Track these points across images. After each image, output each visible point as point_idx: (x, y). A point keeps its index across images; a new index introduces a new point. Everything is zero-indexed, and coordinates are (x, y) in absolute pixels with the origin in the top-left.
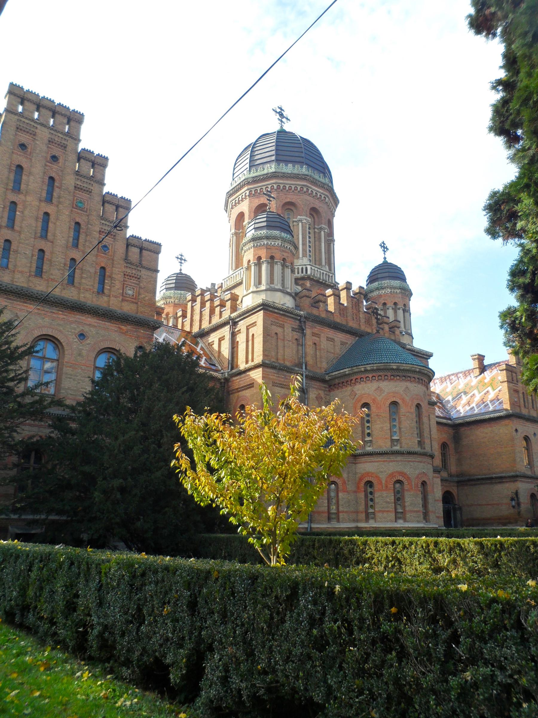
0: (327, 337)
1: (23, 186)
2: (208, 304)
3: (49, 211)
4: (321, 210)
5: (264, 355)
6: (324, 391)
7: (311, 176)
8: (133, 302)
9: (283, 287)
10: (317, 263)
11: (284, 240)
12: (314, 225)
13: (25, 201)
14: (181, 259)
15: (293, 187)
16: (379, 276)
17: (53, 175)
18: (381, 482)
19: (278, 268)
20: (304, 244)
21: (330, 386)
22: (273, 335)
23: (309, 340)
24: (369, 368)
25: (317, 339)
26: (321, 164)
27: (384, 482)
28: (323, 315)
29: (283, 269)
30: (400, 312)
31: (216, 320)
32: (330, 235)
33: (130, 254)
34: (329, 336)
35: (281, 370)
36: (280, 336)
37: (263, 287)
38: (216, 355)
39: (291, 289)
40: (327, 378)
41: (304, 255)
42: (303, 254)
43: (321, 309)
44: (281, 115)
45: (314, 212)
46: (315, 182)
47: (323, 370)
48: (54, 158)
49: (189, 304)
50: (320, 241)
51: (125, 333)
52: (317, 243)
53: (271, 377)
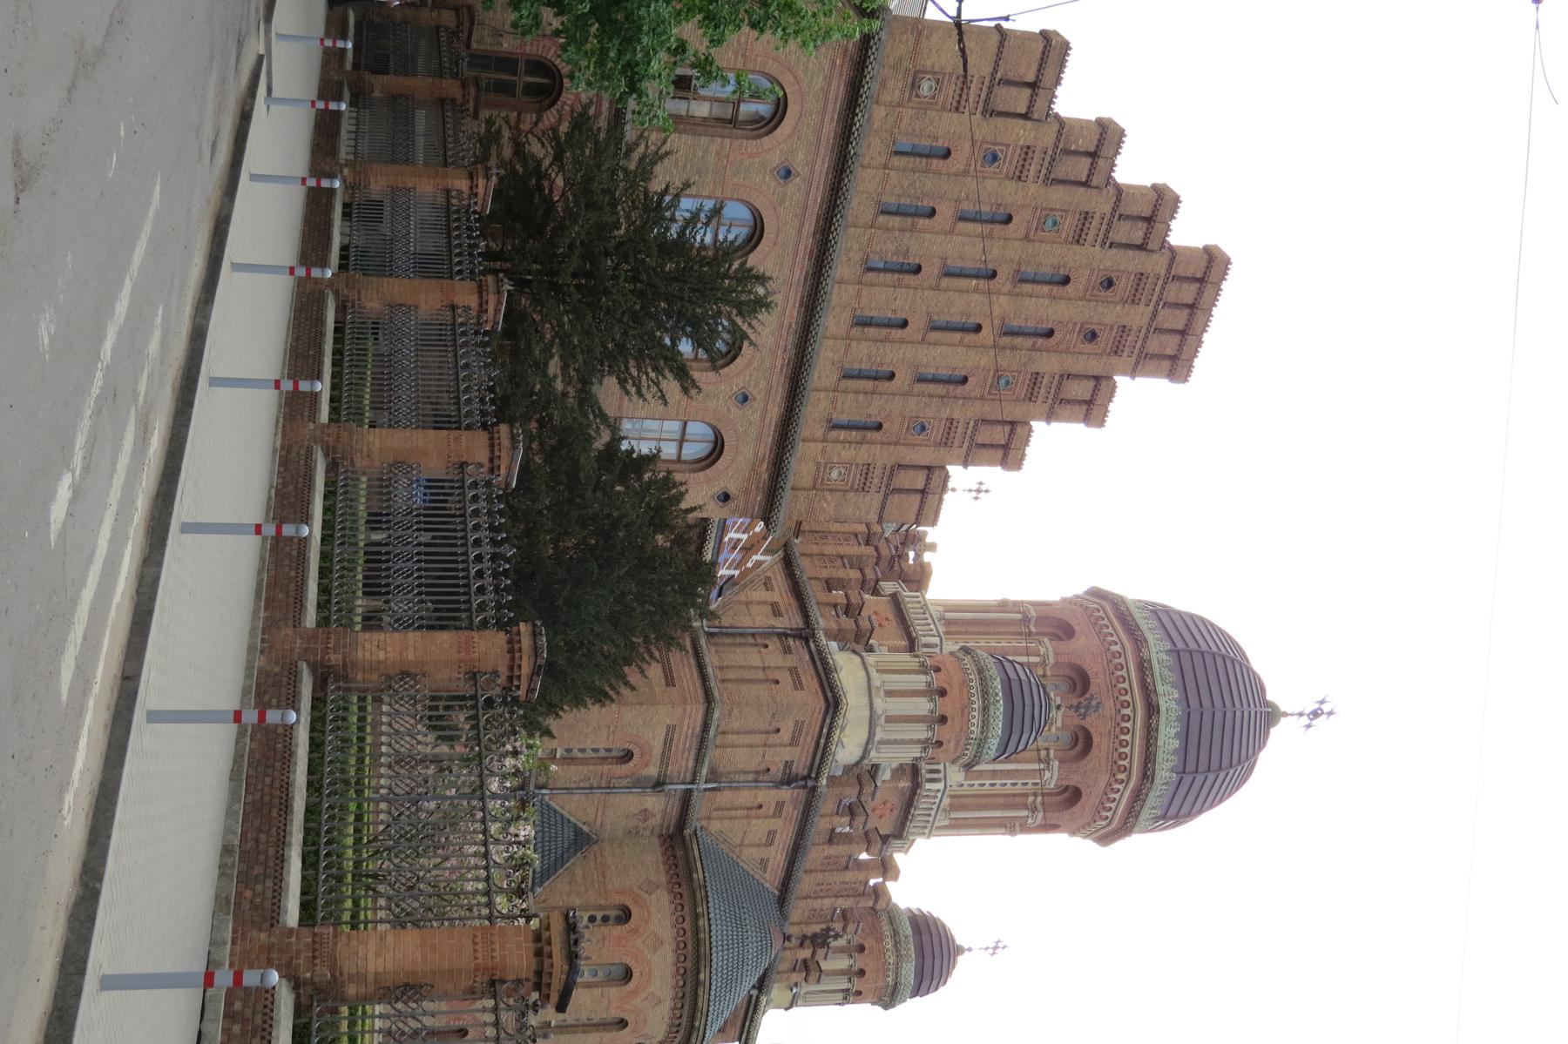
0: (775, 832)
1: (1028, 288)
2: (854, 574)
3: (984, 332)
4: (1077, 809)
6: (661, 826)
8: (816, 479)
9: (881, 742)
11: (981, 743)
13: (998, 293)
15: (1127, 750)
16: (926, 938)
17: (1057, 336)
19: (921, 732)
21: (671, 837)
22: (775, 725)
23: (769, 797)
24: (701, 922)
26: (1185, 810)
29: (919, 742)
30: (844, 984)
32: (1025, 829)
33: (911, 473)
36: (773, 739)
37: (880, 704)
38: (743, 597)
40: (687, 832)
43: (836, 819)
44: (1315, 714)
47: (704, 823)
48: (1093, 336)
50: (1006, 807)
51: (753, 469)
52: (1002, 800)
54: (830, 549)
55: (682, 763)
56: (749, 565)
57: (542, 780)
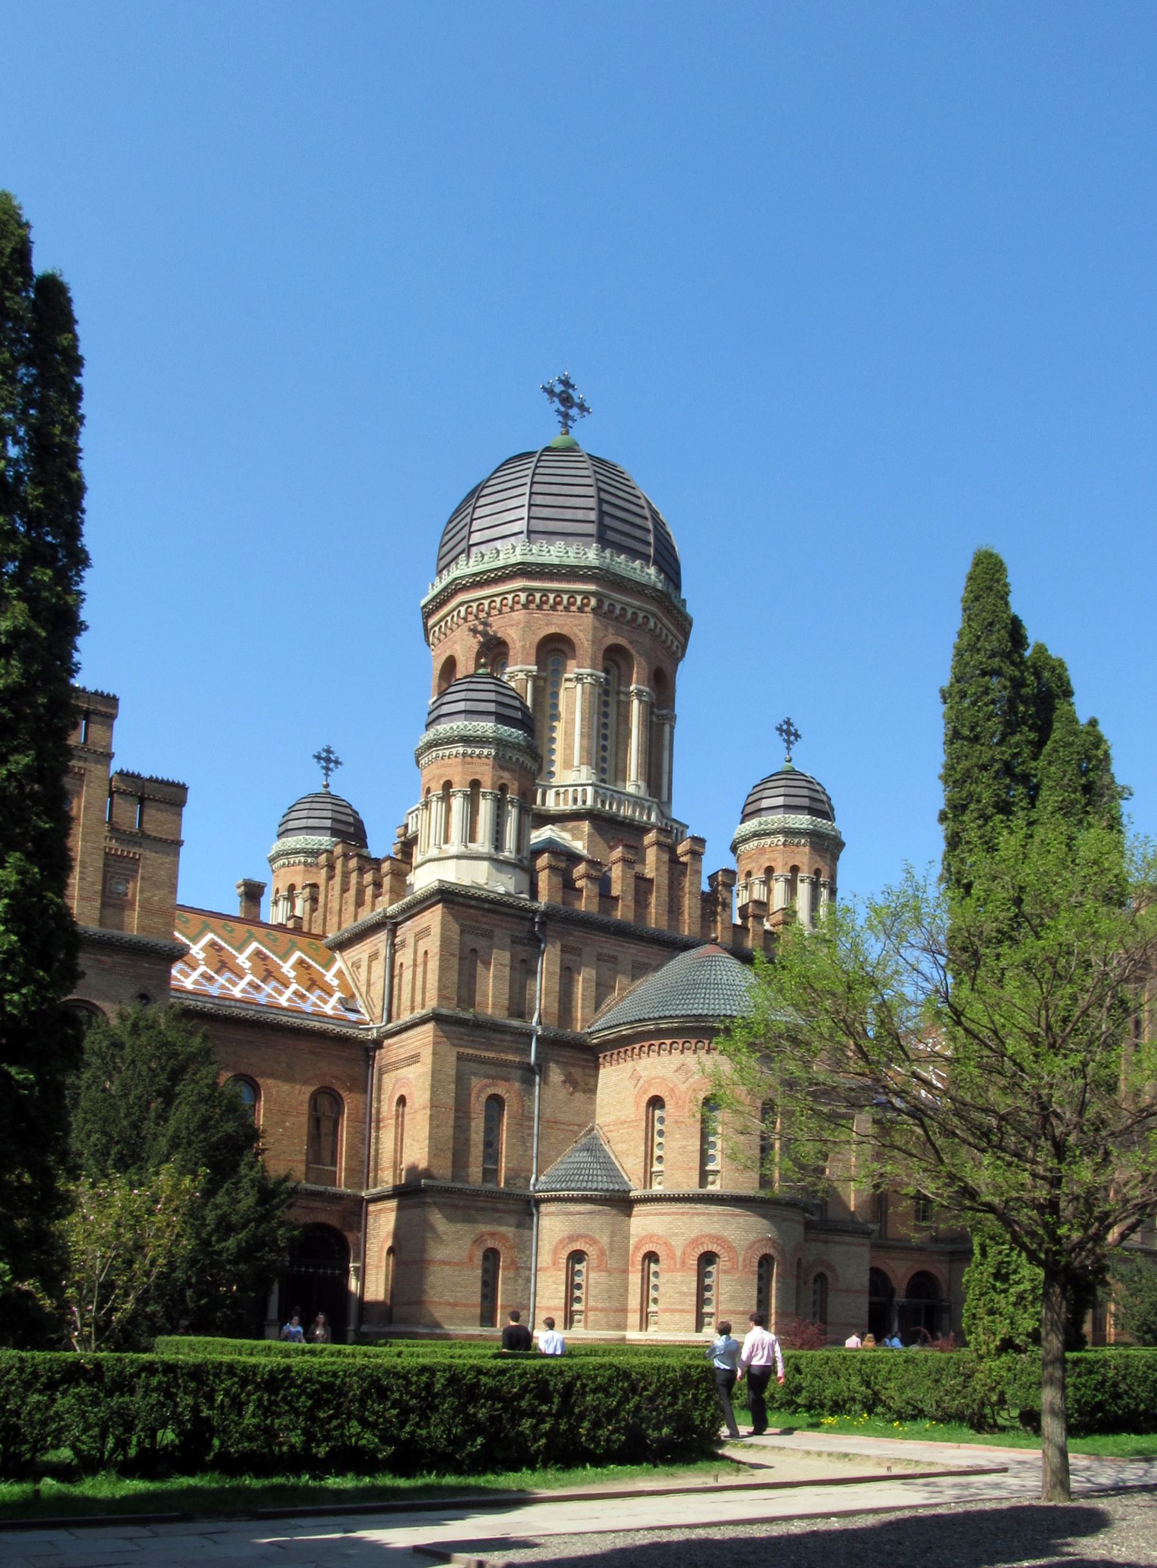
2: (354, 877)
5: (442, 997)
12: (619, 684)
14: (328, 760)
16: (765, 804)
18: (674, 1254)
25: (574, 958)
27: (678, 1254)
31: (367, 915)
34: (605, 951)
37: (455, 847)
38: (364, 989)
39: (519, 849)
42: (581, 758)
49: (324, 871)
54: (335, 905)
56: (335, 982)
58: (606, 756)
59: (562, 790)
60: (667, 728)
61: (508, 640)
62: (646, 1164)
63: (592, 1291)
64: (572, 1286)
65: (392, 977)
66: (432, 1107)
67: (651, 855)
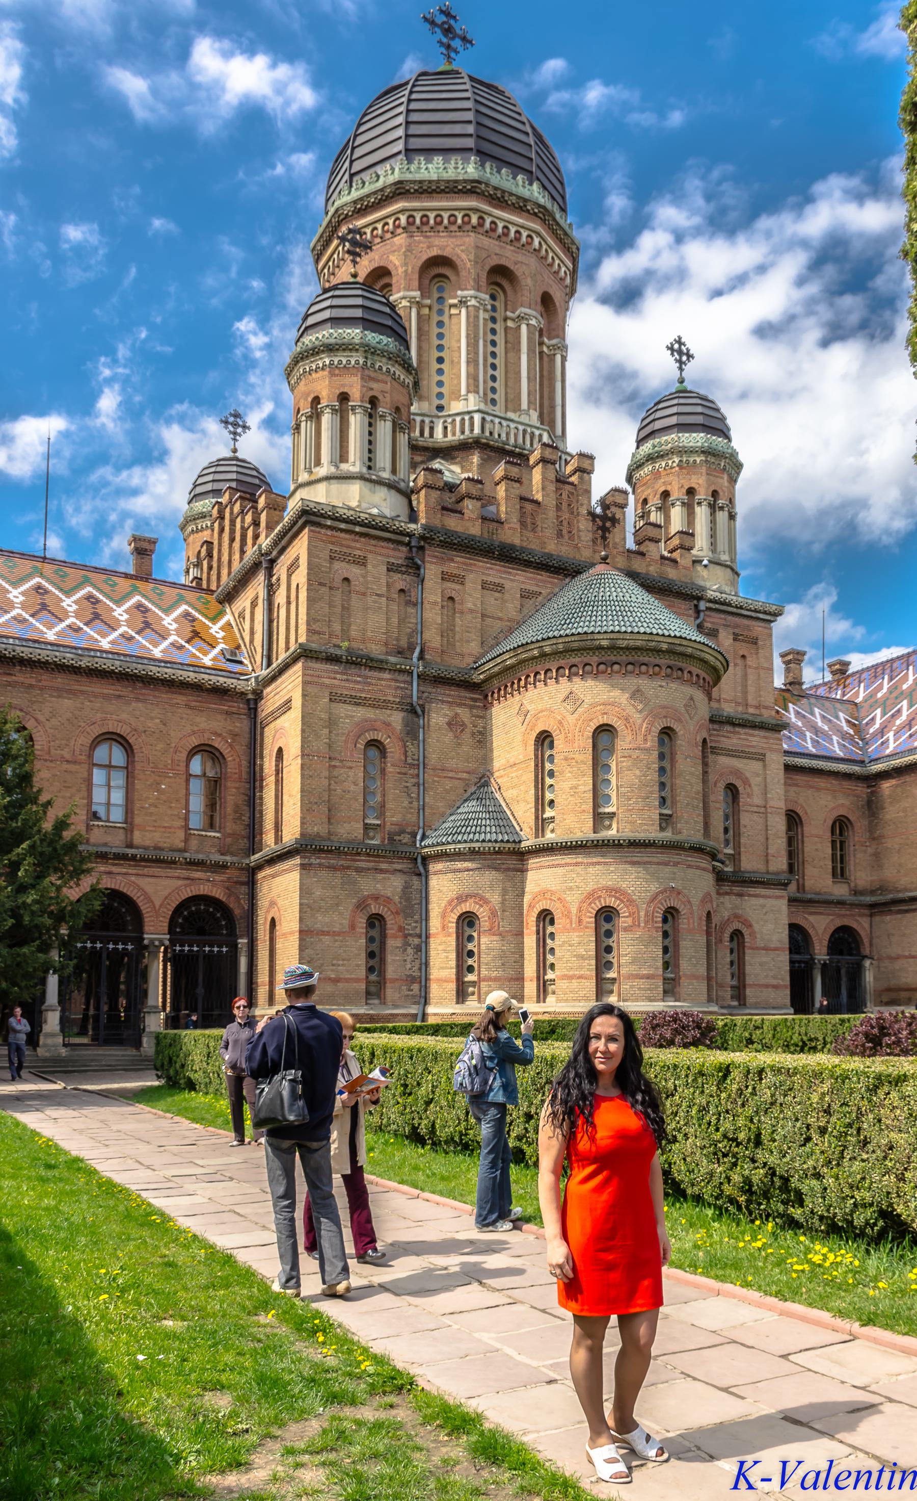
4: (518, 270)
6: (472, 707)
7: (487, 185)
10: (510, 406)
12: (506, 310)
20: (472, 361)
25: (457, 587)
28: (475, 529)
34: (490, 579)
35: (353, 663)
41: (473, 387)
45: (500, 277)
46: (499, 199)
50: (519, 351)
53: (327, 681)
55: (384, 685)
57: (406, 838)
58: (493, 382)
59: (449, 420)
60: (558, 358)
61: (390, 267)
62: (537, 810)
63: (485, 959)
64: (464, 954)
65: (270, 621)
66: (303, 756)
67: (537, 475)
